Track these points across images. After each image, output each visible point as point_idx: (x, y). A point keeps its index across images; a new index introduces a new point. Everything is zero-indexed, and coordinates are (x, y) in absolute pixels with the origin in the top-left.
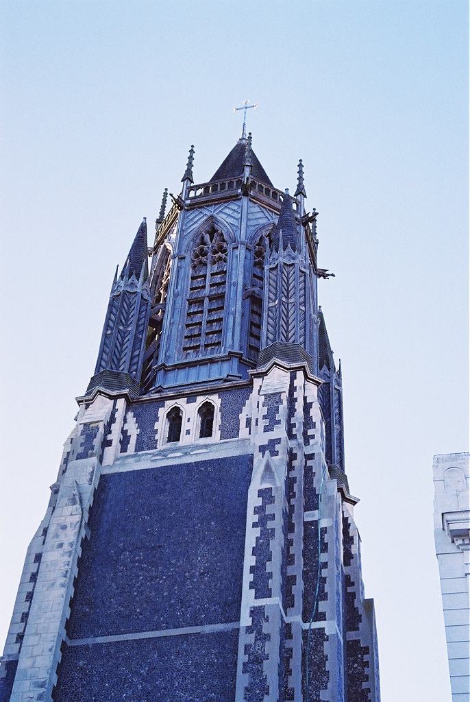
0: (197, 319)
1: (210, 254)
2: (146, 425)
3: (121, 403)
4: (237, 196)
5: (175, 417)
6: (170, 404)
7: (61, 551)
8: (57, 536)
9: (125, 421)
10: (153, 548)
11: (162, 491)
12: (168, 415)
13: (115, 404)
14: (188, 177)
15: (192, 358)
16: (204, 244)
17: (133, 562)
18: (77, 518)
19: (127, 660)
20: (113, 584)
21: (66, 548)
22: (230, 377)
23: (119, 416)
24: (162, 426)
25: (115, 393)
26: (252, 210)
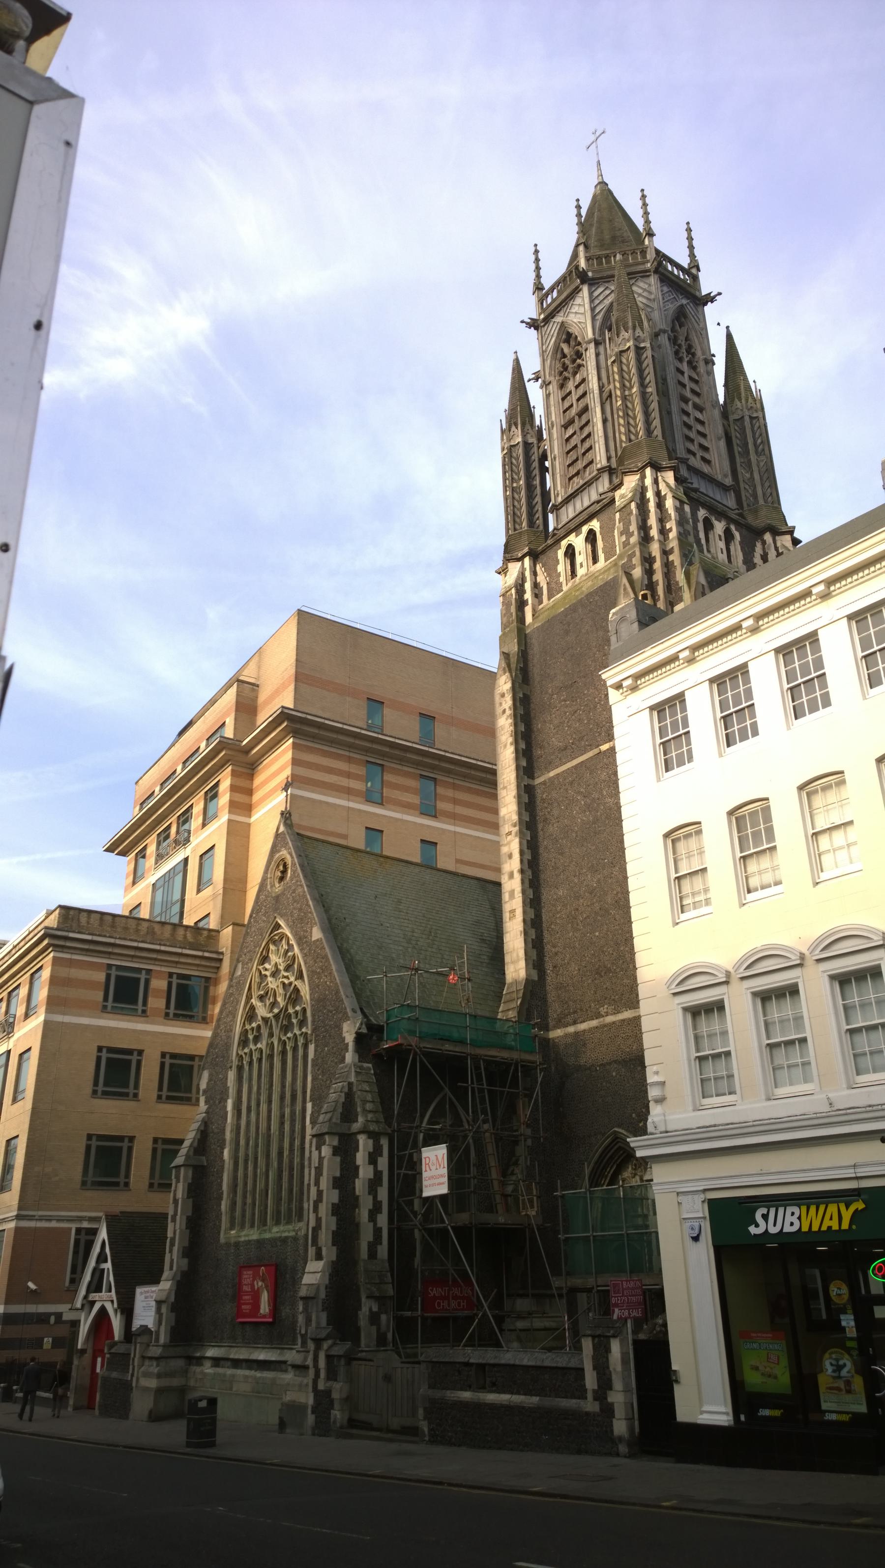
0: (573, 442)
1: (571, 366)
2: (551, 571)
3: (527, 560)
4: (577, 287)
5: (570, 552)
6: (564, 543)
7: (505, 716)
8: (501, 704)
9: (534, 573)
10: (571, 686)
11: (567, 632)
12: (566, 554)
13: (523, 564)
14: (538, 287)
15: (578, 482)
16: (564, 356)
17: (560, 702)
18: (509, 685)
19: (571, 783)
20: (551, 726)
21: (508, 712)
22: (603, 497)
23: (528, 574)
24: (562, 567)
25: (520, 555)
26: (596, 294)
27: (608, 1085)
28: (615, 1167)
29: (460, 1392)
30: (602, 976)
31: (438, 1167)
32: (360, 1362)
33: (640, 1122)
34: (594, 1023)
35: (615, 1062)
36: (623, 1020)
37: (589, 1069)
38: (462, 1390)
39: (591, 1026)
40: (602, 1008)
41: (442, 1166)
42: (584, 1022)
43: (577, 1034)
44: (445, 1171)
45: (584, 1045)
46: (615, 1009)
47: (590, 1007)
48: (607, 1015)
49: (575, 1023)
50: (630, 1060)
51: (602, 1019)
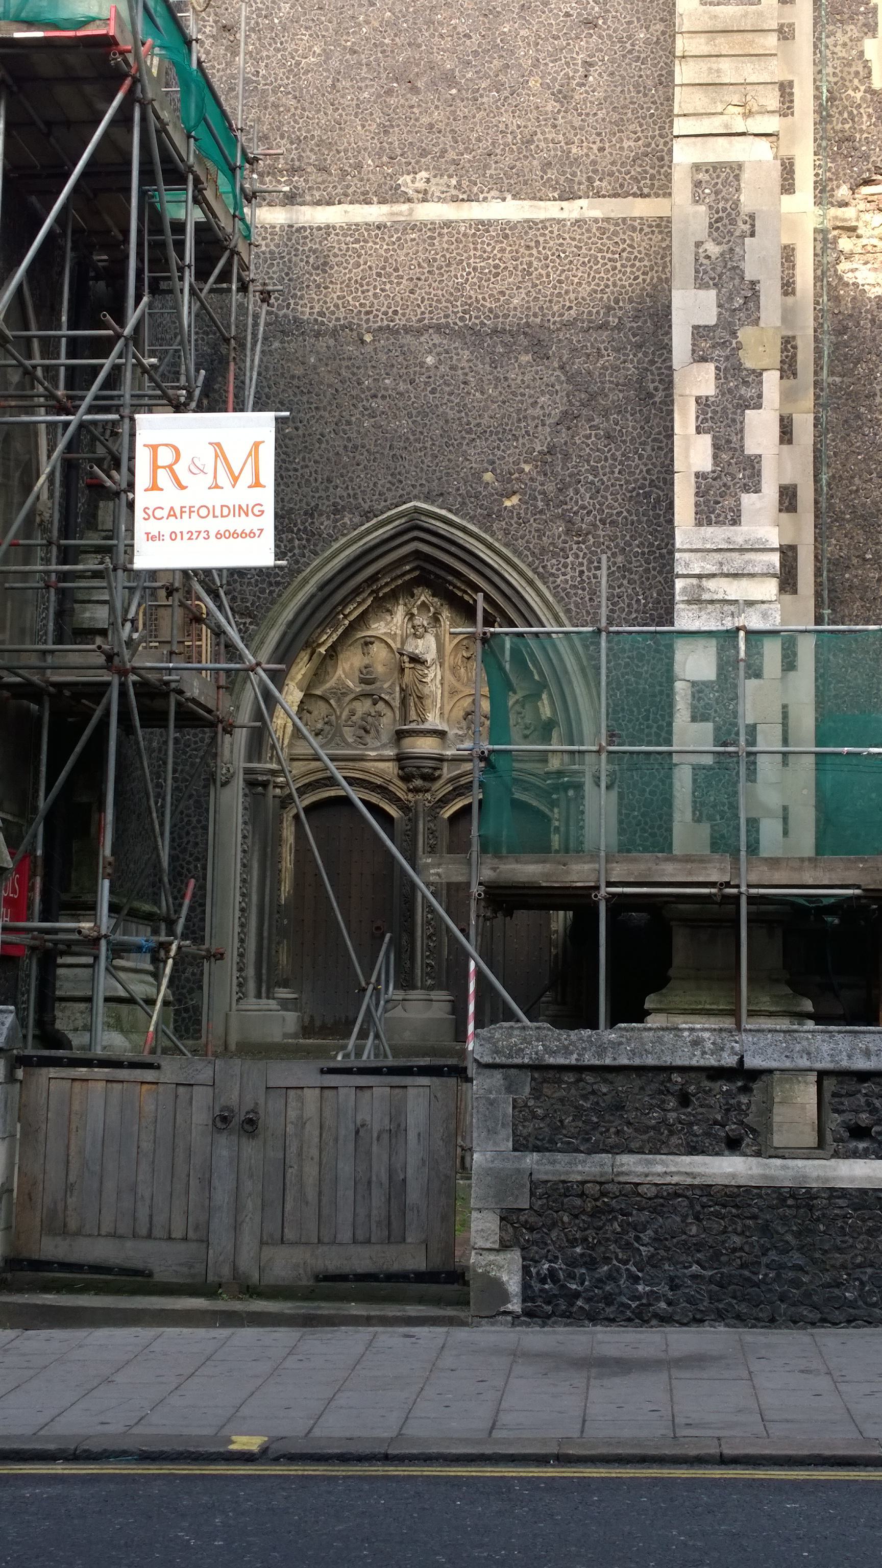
27: (402, 387)
28: (369, 602)
29: (687, 1159)
30: (414, 90)
31: (223, 478)
32: (83, 1071)
33: (508, 497)
34: (375, 213)
35: (438, 328)
36: (484, 225)
37: (334, 333)
38: (693, 1150)
39: (358, 219)
40: (408, 178)
41: (247, 477)
42: (329, 203)
43: (293, 231)
44: (267, 497)
45: (323, 267)
46: (458, 186)
47: (359, 166)
48: (424, 200)
49: (291, 199)
50: (495, 331)
51: (405, 207)
